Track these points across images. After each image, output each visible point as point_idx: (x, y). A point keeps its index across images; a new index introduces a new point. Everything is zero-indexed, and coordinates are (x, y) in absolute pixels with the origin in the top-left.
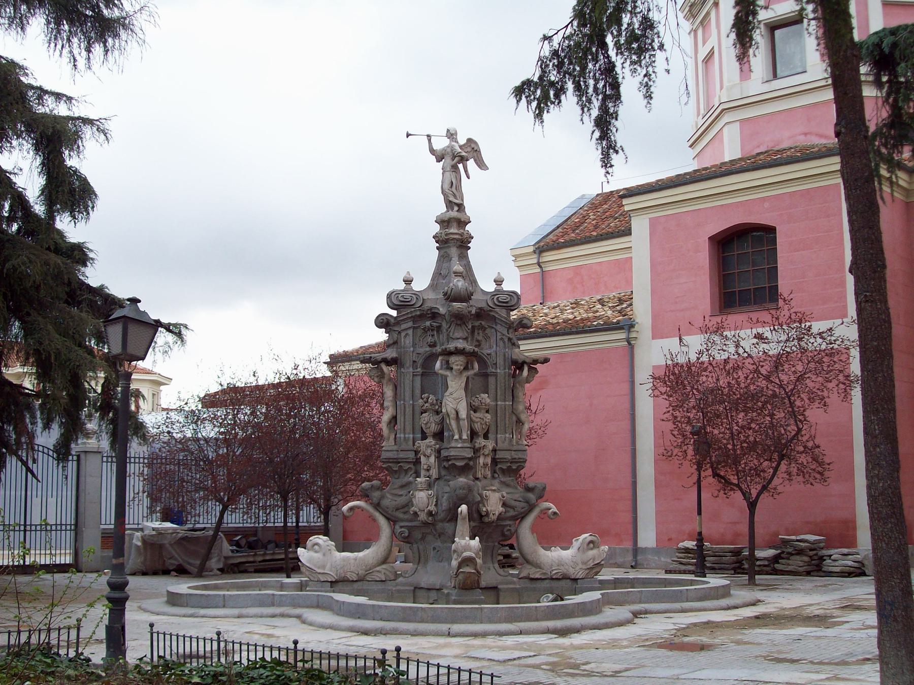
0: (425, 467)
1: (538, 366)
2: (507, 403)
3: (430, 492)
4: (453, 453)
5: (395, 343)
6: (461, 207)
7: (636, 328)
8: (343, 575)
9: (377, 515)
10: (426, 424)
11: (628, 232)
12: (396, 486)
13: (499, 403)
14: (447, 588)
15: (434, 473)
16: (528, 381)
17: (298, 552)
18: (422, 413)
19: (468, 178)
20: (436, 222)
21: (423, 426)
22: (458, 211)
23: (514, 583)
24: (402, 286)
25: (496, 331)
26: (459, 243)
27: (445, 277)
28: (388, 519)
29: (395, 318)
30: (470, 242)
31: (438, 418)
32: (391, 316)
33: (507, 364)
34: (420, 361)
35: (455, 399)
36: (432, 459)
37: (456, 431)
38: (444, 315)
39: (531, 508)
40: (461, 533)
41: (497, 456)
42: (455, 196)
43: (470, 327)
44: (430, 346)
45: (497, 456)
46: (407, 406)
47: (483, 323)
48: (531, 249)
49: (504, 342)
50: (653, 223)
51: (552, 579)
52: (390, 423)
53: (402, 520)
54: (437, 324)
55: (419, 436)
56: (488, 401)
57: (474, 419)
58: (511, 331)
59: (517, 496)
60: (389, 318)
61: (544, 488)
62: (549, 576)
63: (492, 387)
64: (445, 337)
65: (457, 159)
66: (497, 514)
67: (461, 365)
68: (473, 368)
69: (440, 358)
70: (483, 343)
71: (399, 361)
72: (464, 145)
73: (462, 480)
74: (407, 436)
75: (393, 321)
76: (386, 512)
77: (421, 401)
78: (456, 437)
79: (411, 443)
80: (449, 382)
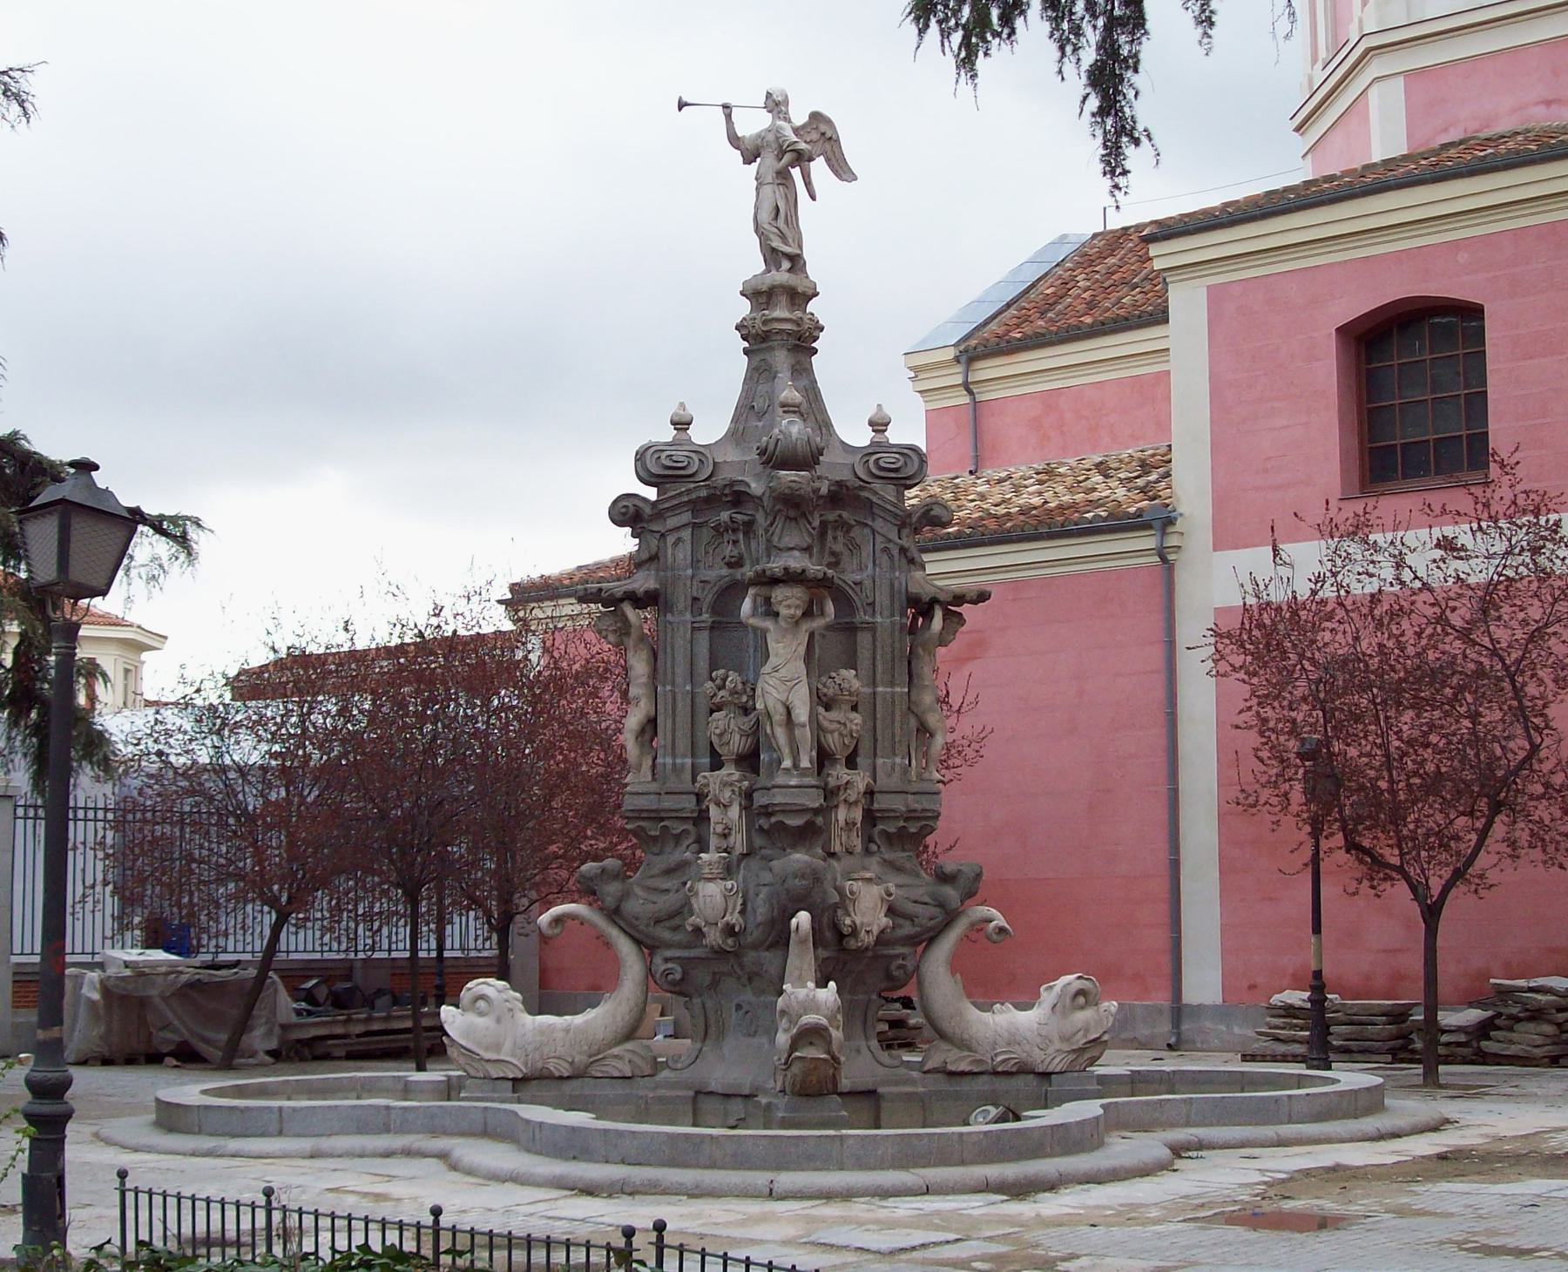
0: (719, 829)
1: (965, 610)
2: (898, 689)
3: (729, 884)
4: (779, 798)
5: (653, 558)
6: (796, 262)
7: (1178, 527)
8: (539, 1065)
9: (614, 933)
10: (721, 735)
11: (1160, 317)
12: (656, 871)
13: (880, 689)
14: (766, 1092)
15: (738, 842)
16: (942, 641)
17: (442, 1015)
18: (712, 712)
19: (813, 198)
20: (742, 294)
21: (715, 740)
22: (790, 270)
23: (913, 1082)
24: (668, 434)
25: (873, 531)
26: (793, 341)
27: (761, 415)
28: (638, 942)
29: (654, 504)
30: (816, 339)
31: (746, 723)
32: (645, 500)
33: (897, 605)
34: (708, 598)
35: (784, 682)
36: (734, 812)
37: (786, 751)
38: (760, 498)
39: (950, 918)
40: (796, 973)
41: (876, 806)
42: (783, 238)
43: (816, 523)
44: (730, 565)
45: (876, 806)
46: (679, 697)
47: (845, 515)
48: (950, 354)
49: (891, 557)
50: (1216, 297)
51: (996, 1073)
52: (641, 732)
53: (669, 946)
54: (746, 518)
55: (706, 761)
56: (856, 684)
57: (825, 724)
58: (905, 531)
59: (919, 893)
60: (640, 504)
61: (979, 876)
62: (989, 1068)
63: (864, 654)
64: (763, 547)
65: (787, 158)
66: (876, 931)
67: (797, 607)
68: (822, 614)
69: (751, 591)
70: (845, 558)
71: (661, 599)
72: (804, 127)
73: (799, 858)
74: (678, 761)
75: (648, 510)
76: (635, 927)
77: (709, 684)
78: (787, 763)
79: (688, 776)
80: (771, 645)
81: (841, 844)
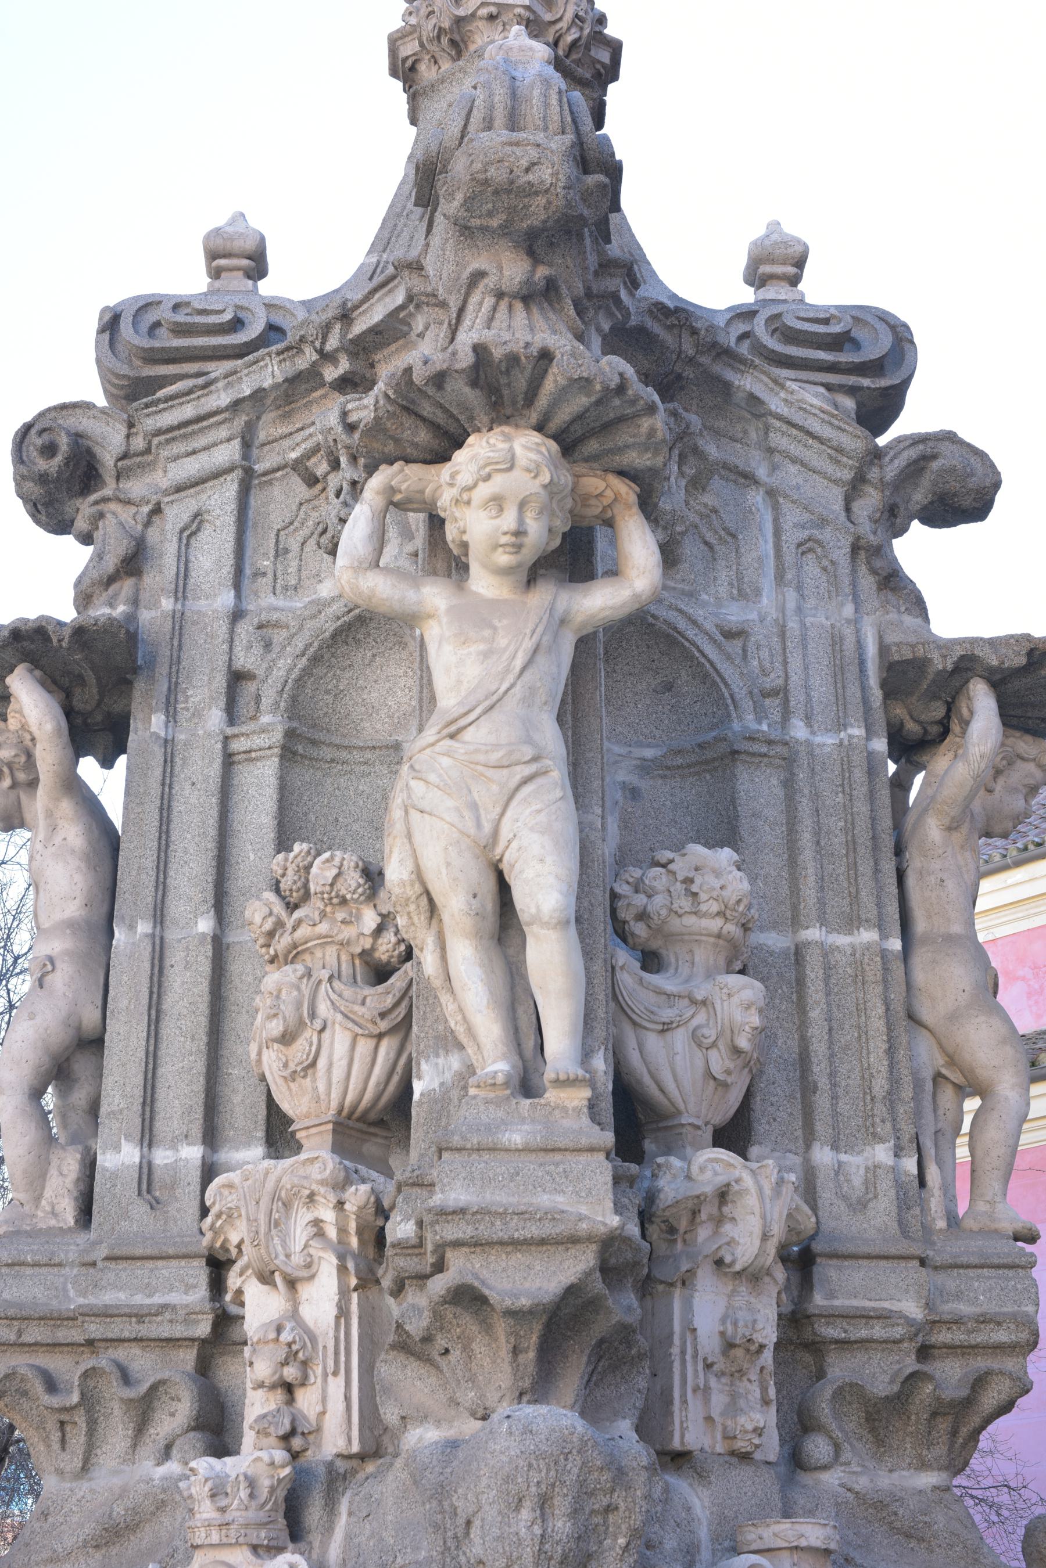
25: (771, 493)
45: (819, 1299)
46: (175, 957)
74: (162, 1157)
81: (709, 1419)
